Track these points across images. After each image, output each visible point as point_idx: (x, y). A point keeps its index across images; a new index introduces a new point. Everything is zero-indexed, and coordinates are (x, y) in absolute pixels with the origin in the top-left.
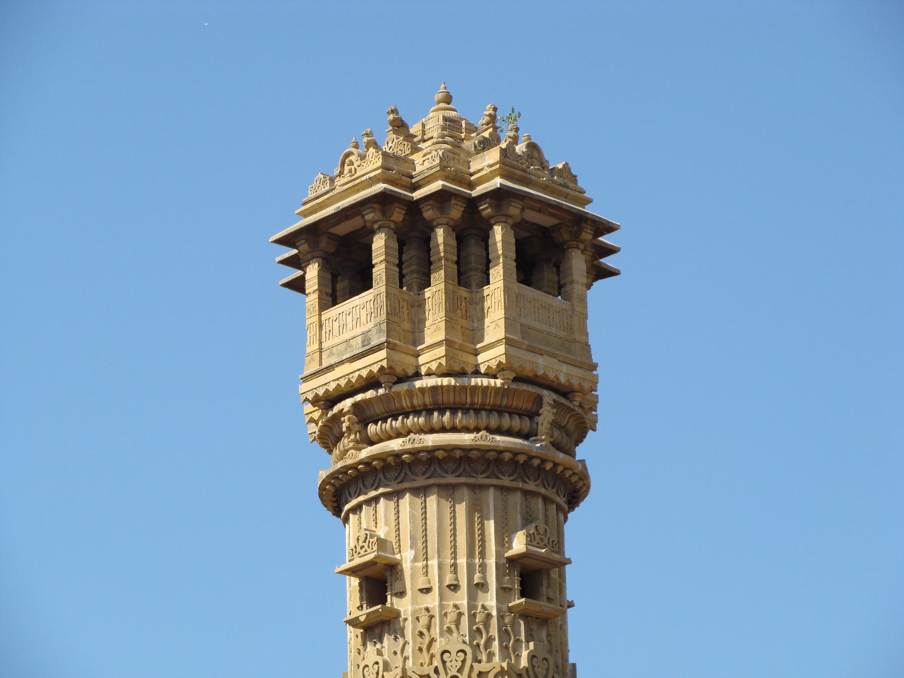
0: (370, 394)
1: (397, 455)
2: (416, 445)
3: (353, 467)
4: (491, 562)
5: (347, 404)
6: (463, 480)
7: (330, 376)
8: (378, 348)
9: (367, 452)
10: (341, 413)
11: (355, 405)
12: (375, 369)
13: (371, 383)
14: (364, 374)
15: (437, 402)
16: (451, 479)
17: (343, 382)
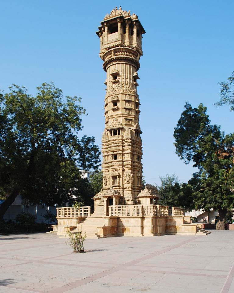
0: (116, 48)
1: (121, 57)
2: (124, 56)
3: (113, 59)
4: (132, 76)
5: (113, 49)
6: (129, 63)
7: (110, 44)
8: (119, 40)
9: (116, 57)
10: (112, 50)
11: (114, 49)
12: (119, 44)
13: (117, 46)
14: (117, 44)
15: (127, 50)
16: (127, 63)
17: (112, 46)
